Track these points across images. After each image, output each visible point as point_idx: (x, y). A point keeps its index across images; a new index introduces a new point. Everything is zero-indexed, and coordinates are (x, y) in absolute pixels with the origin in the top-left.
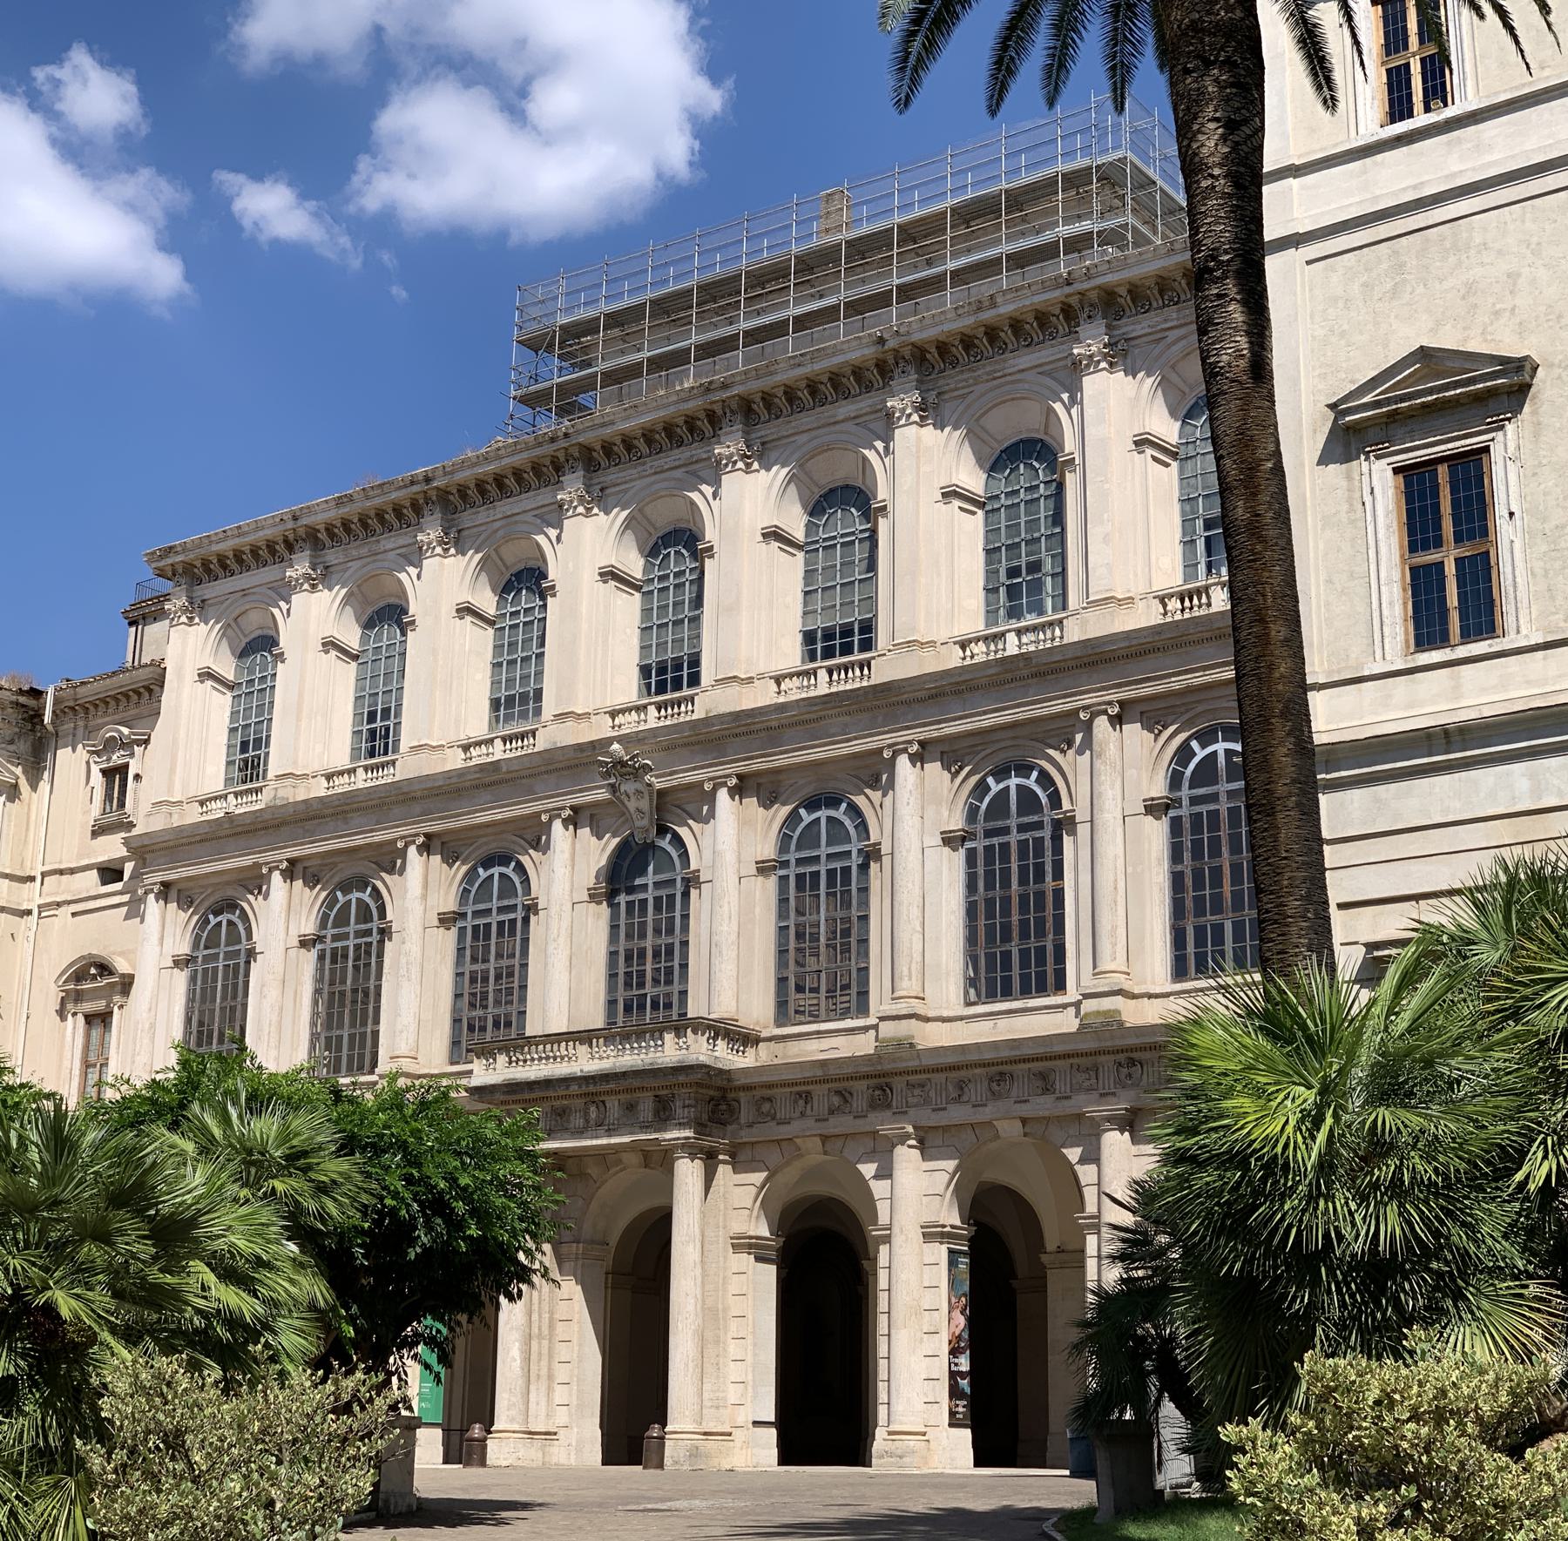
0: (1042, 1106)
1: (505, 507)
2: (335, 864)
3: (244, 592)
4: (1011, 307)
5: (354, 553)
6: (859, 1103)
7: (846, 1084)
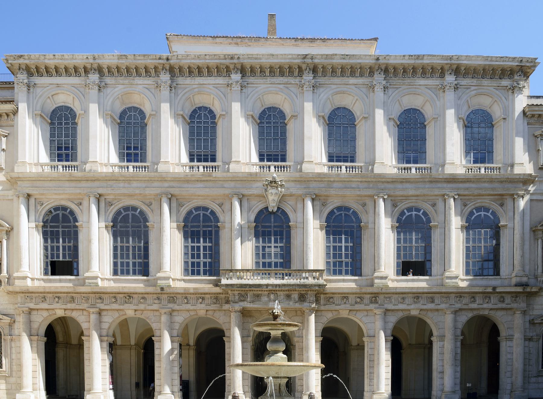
0: (431, 306)
1: (199, 80)
2: (121, 200)
3: (58, 85)
4: (428, 62)
5: (121, 82)
6: (366, 301)
7: (362, 295)
